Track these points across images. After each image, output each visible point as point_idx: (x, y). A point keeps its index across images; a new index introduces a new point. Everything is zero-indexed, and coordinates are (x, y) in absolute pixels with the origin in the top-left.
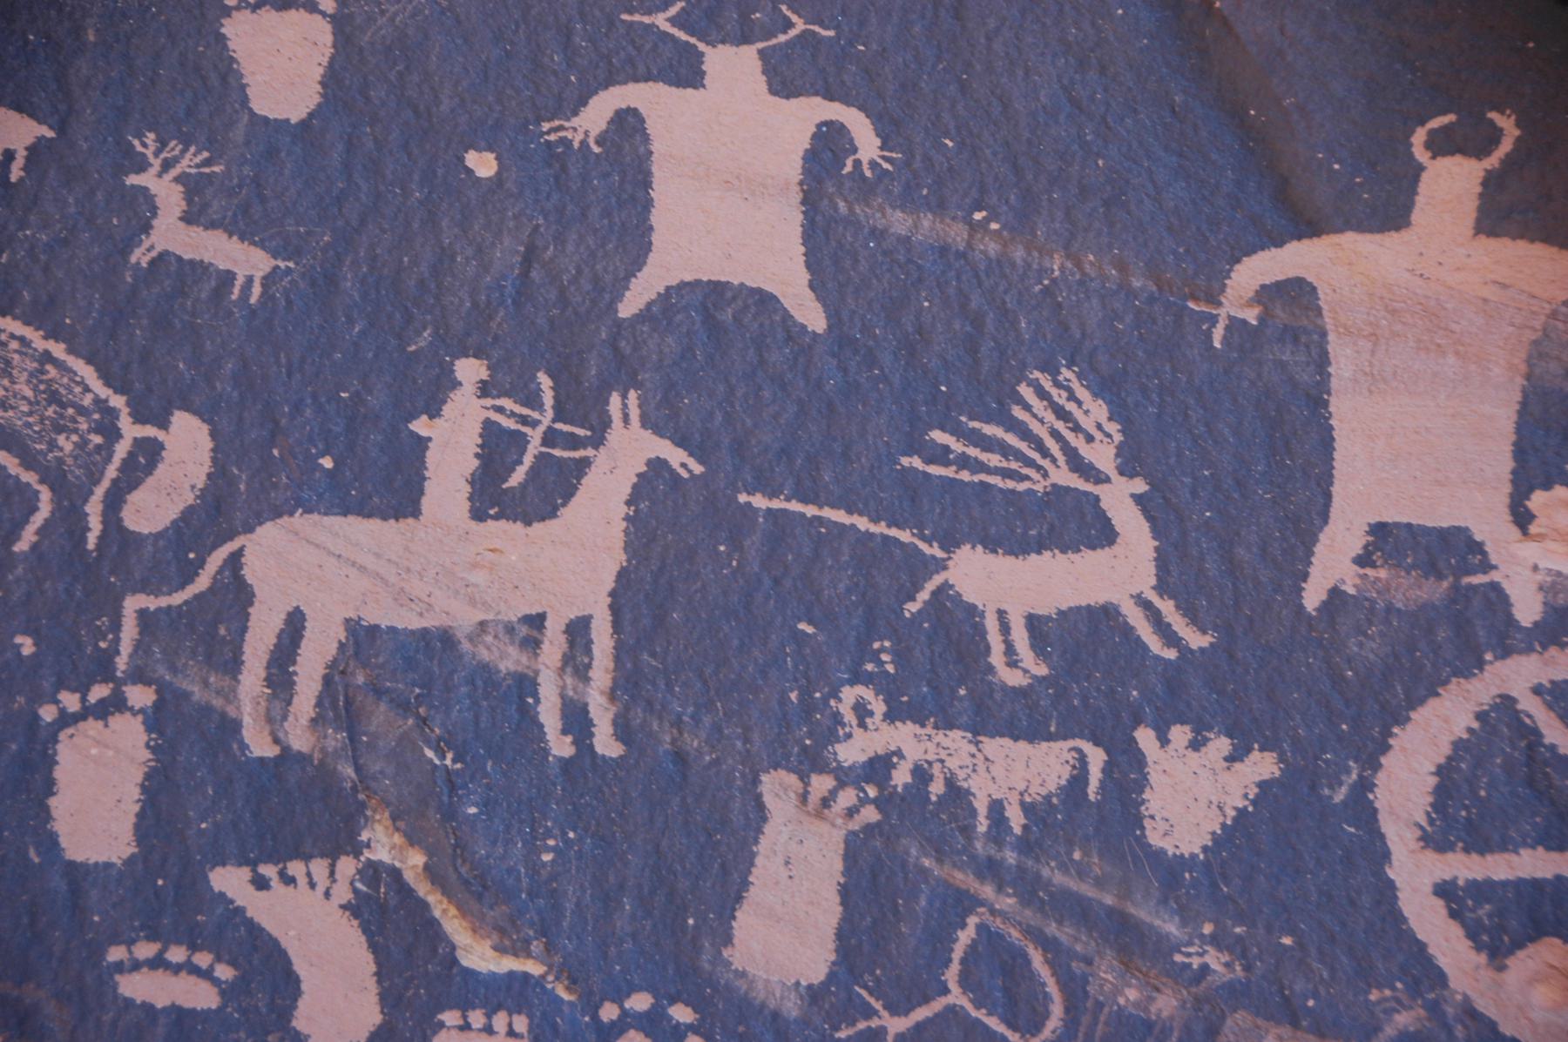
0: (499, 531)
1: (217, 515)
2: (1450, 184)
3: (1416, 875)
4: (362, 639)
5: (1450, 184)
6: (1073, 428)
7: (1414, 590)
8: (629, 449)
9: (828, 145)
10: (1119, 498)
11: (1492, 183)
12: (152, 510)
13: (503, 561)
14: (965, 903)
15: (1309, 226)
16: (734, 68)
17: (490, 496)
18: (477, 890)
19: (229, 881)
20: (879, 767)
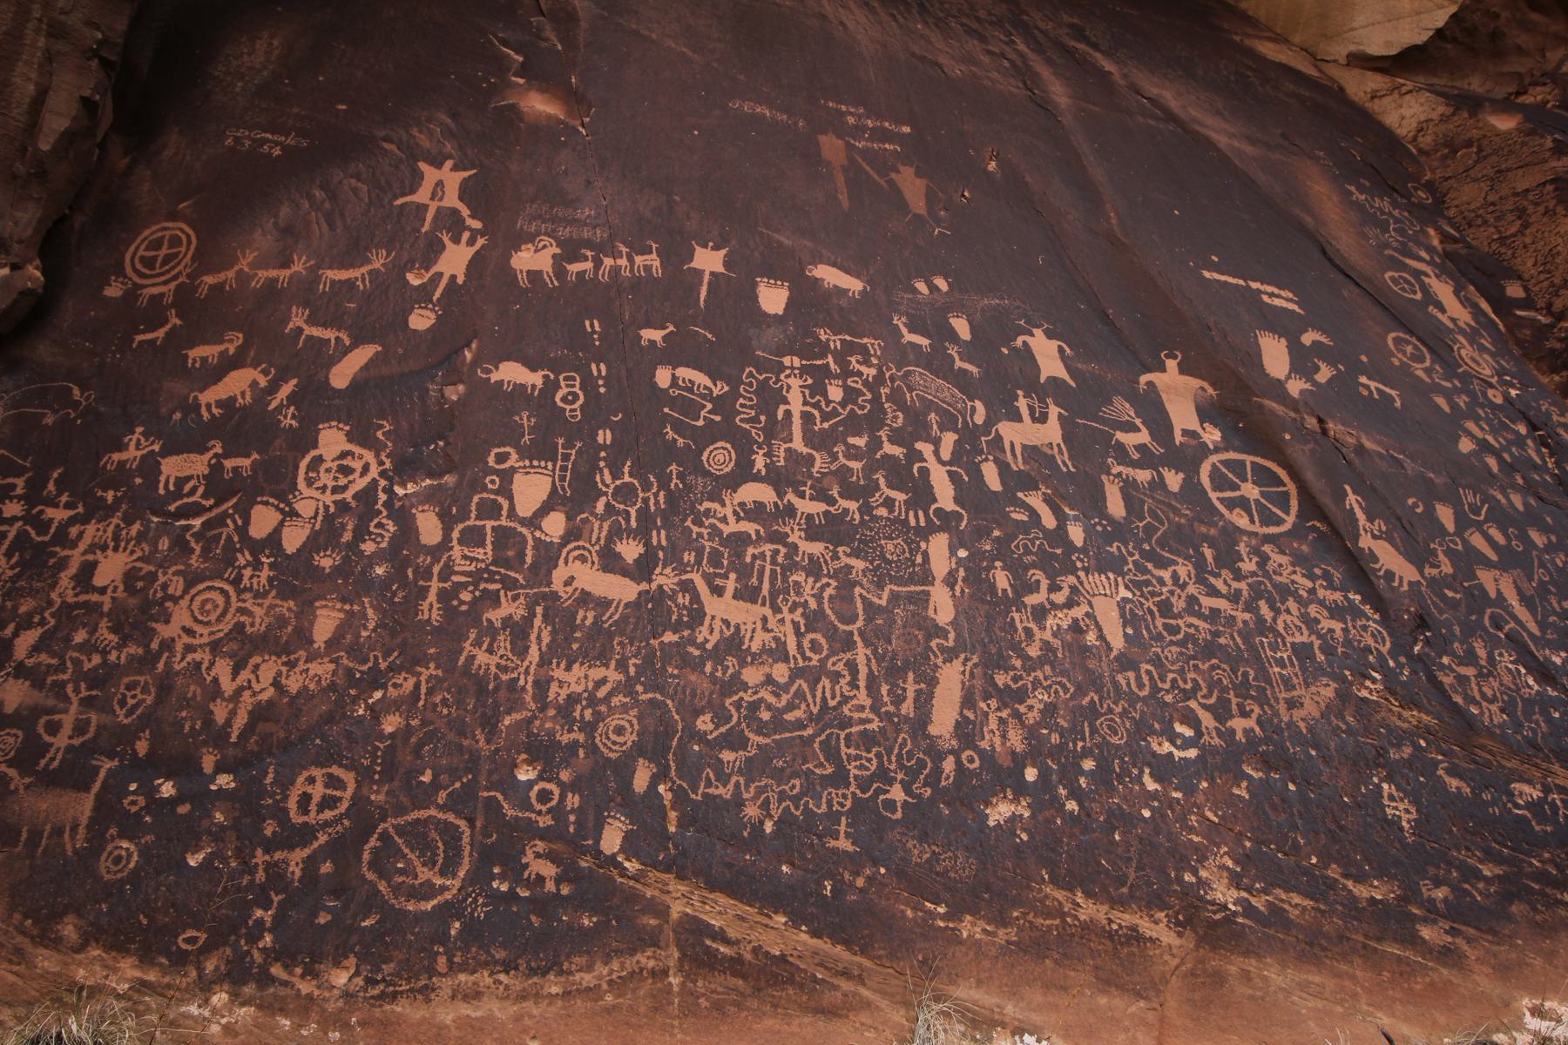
0: (1038, 425)
1: (990, 422)
2: (1171, 364)
3: (1213, 496)
4: (1024, 447)
5: (1171, 364)
6: (1123, 409)
7: (1193, 442)
8: (1054, 411)
9: (1061, 350)
10: (1138, 422)
11: (1179, 364)
12: (980, 418)
13: (1034, 431)
14: (1143, 502)
15: (1150, 371)
16: (1038, 332)
17: (1034, 420)
18: (1063, 498)
19: (1020, 495)
20: (1119, 475)
